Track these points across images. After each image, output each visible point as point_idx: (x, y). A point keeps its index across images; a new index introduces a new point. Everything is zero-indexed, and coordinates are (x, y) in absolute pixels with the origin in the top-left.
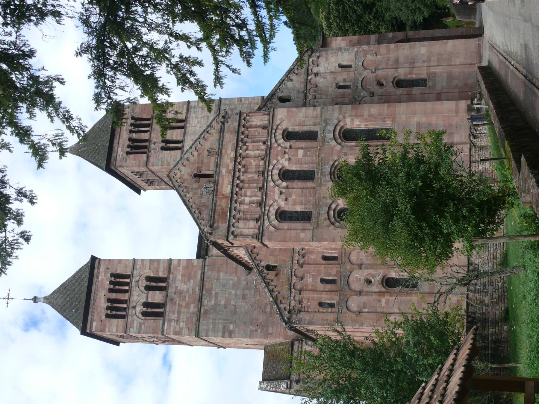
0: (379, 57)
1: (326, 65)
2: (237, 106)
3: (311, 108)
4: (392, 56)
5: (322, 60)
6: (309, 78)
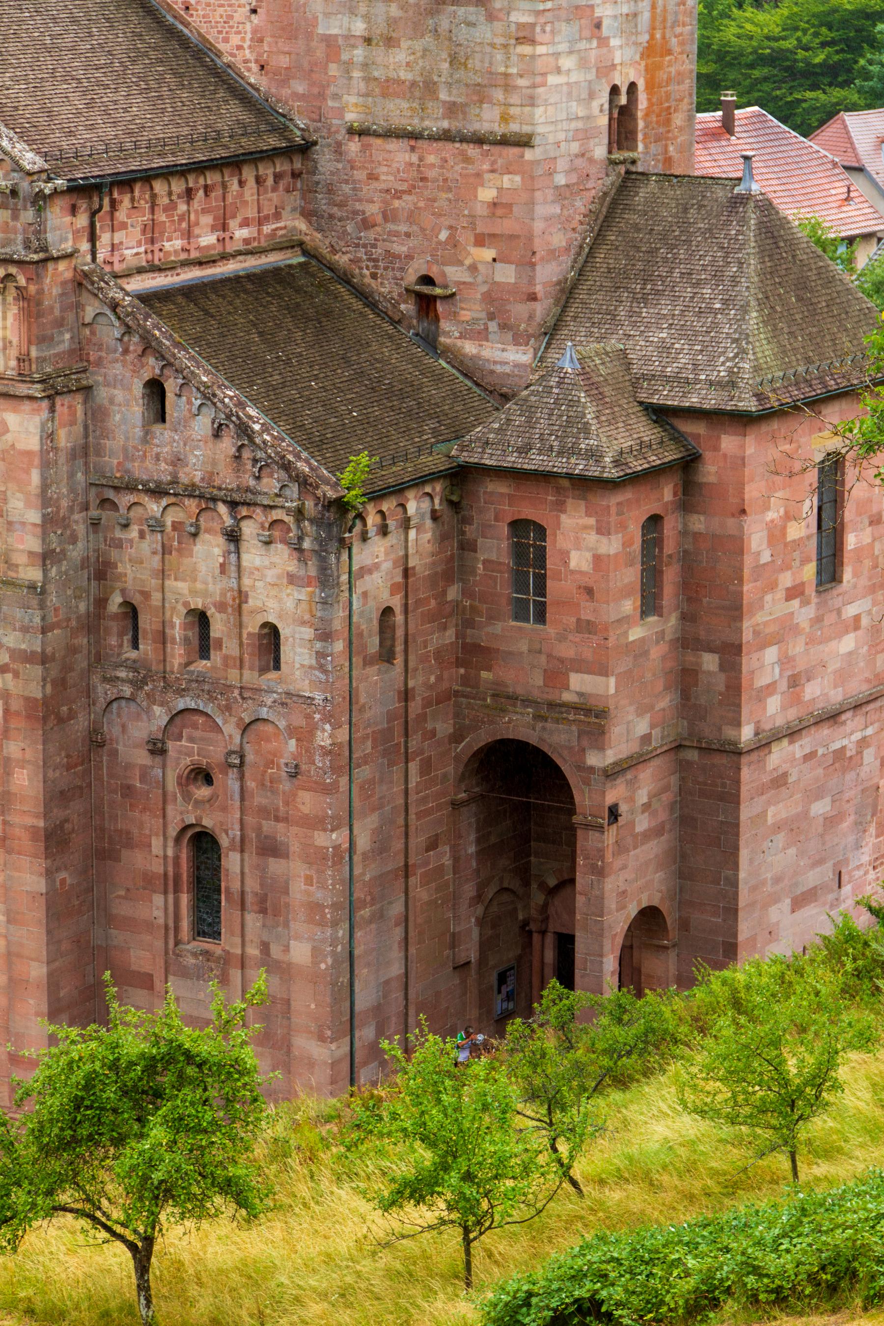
0: (286, 786)
1: (271, 575)
2: (498, 26)
3: (34, 544)
4: (291, 837)
5: (281, 558)
6: (222, 509)
